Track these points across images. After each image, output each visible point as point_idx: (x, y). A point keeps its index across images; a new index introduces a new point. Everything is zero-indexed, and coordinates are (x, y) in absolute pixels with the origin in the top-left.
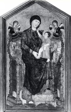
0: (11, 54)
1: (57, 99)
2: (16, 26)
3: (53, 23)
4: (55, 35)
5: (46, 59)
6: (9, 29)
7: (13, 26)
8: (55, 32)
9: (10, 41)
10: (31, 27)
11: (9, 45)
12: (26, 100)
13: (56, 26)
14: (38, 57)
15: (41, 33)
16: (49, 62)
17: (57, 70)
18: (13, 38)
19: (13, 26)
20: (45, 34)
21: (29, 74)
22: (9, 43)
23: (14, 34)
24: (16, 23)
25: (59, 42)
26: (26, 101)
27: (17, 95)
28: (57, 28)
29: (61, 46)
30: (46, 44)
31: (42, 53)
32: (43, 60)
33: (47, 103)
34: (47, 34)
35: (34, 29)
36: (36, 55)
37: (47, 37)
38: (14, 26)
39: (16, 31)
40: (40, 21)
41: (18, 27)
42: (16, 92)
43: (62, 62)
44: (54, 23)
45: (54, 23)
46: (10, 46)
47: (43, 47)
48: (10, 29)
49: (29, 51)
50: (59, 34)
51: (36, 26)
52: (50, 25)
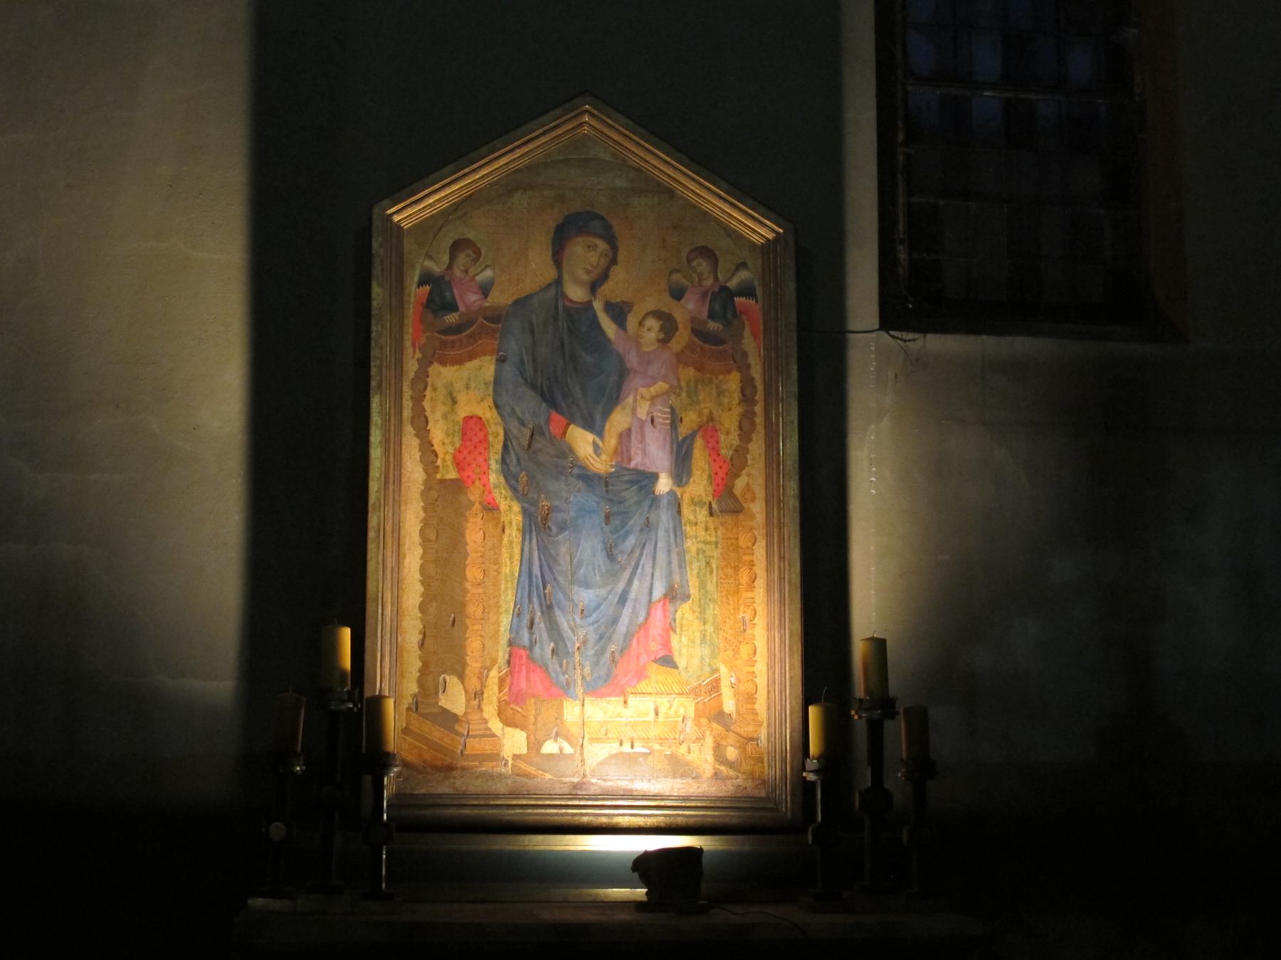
0: (434, 442)
1: (715, 725)
2: (466, 272)
3: (689, 261)
4: (699, 333)
5: (655, 477)
6: (422, 283)
7: (450, 267)
8: (705, 314)
9: (425, 364)
10: (558, 282)
11: (421, 386)
12: (522, 730)
13: (709, 282)
14: (601, 465)
15: (619, 312)
16: (668, 493)
17: (716, 543)
18: (444, 345)
19: (450, 267)
20: (641, 324)
21: (545, 564)
22: (422, 376)
23: (451, 319)
24: (470, 252)
25: (729, 372)
26: (524, 735)
27: (468, 701)
28: (716, 290)
29: (736, 397)
30: (649, 386)
31: (625, 436)
32: (632, 482)
33: (657, 747)
34: (652, 323)
35: (576, 293)
36: (590, 450)
37: (657, 345)
38: (457, 272)
39: (470, 299)
40: (615, 249)
41: (478, 278)
42: (461, 677)
43: (749, 496)
44: (695, 263)
45: (700, 260)
46: (429, 388)
47: (630, 400)
48: (428, 288)
49: (548, 422)
50: (728, 324)
51: (588, 272)
52: (671, 273)
